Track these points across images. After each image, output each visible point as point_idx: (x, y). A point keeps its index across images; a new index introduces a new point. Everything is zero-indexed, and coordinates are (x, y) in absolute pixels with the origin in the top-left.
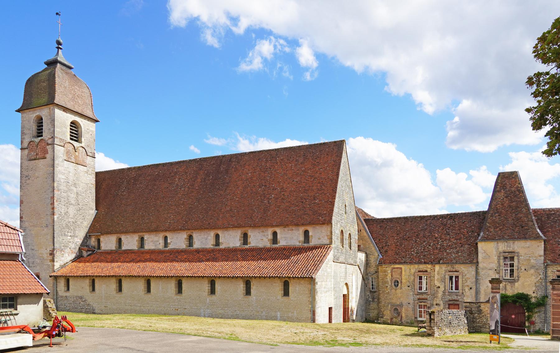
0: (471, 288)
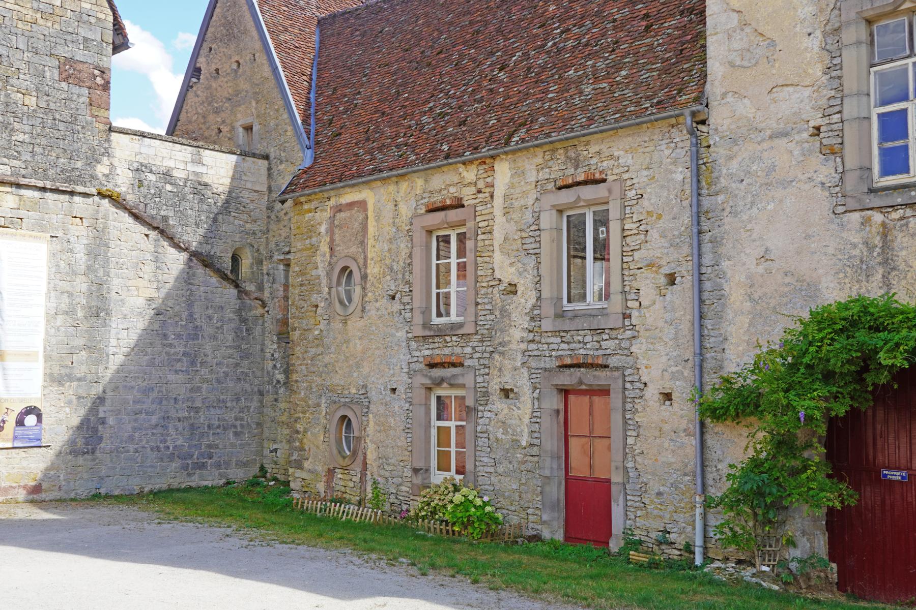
0: (671, 280)
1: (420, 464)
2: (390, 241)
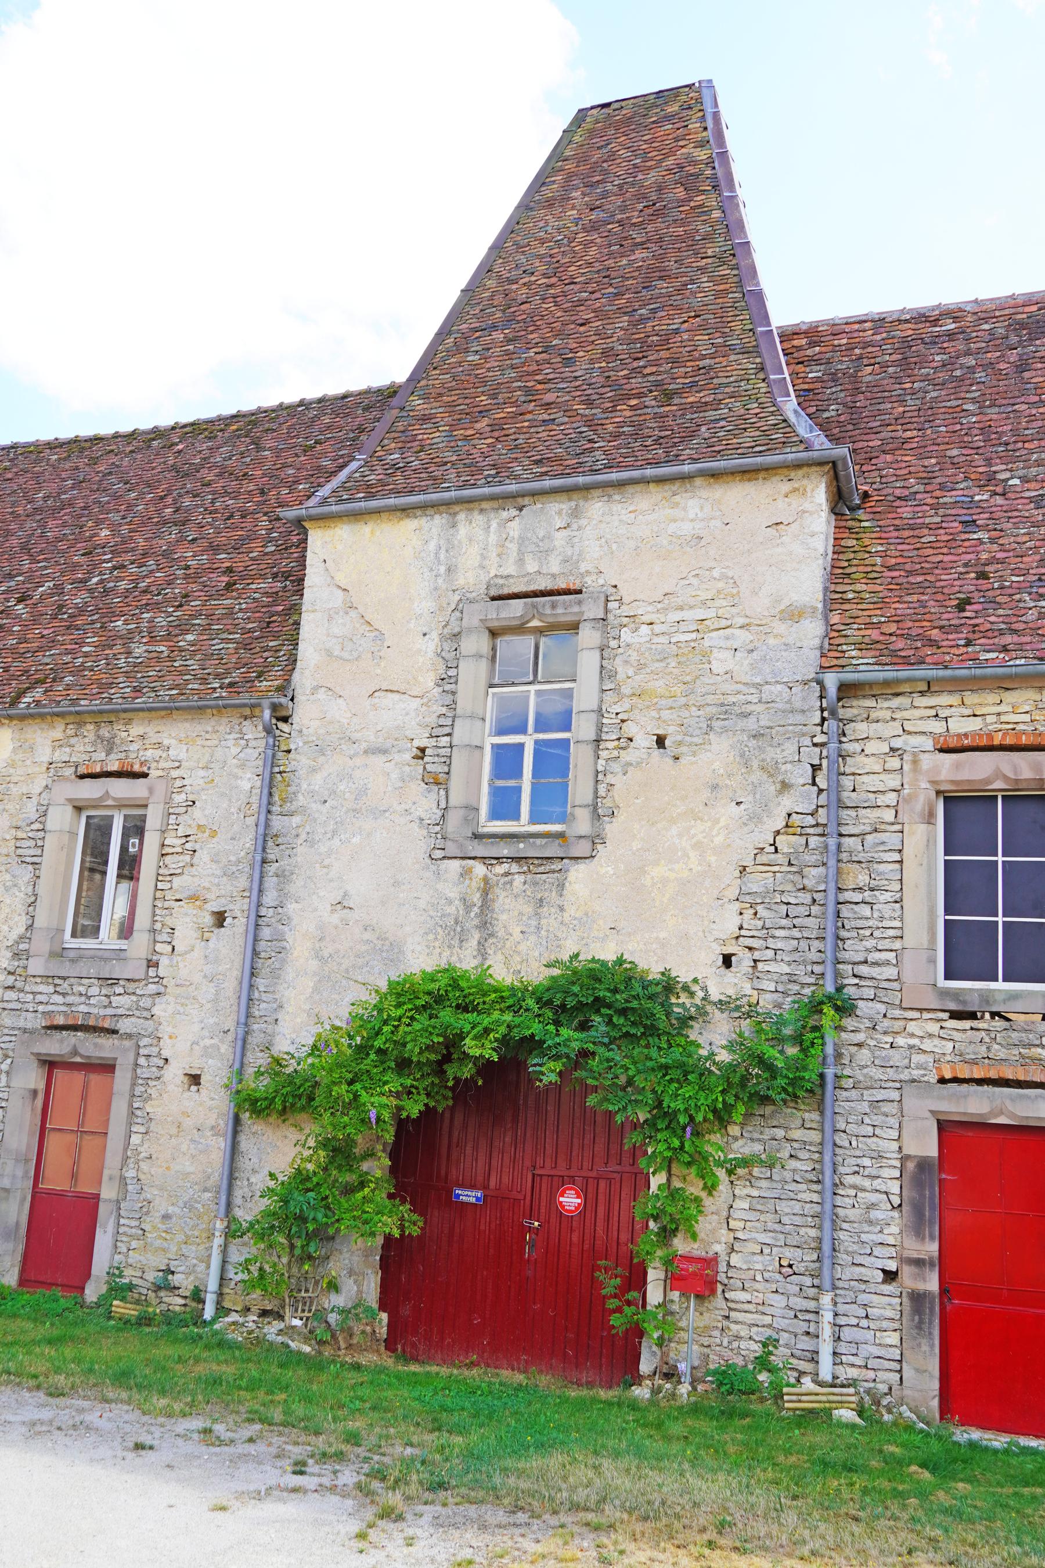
0: (220, 919)
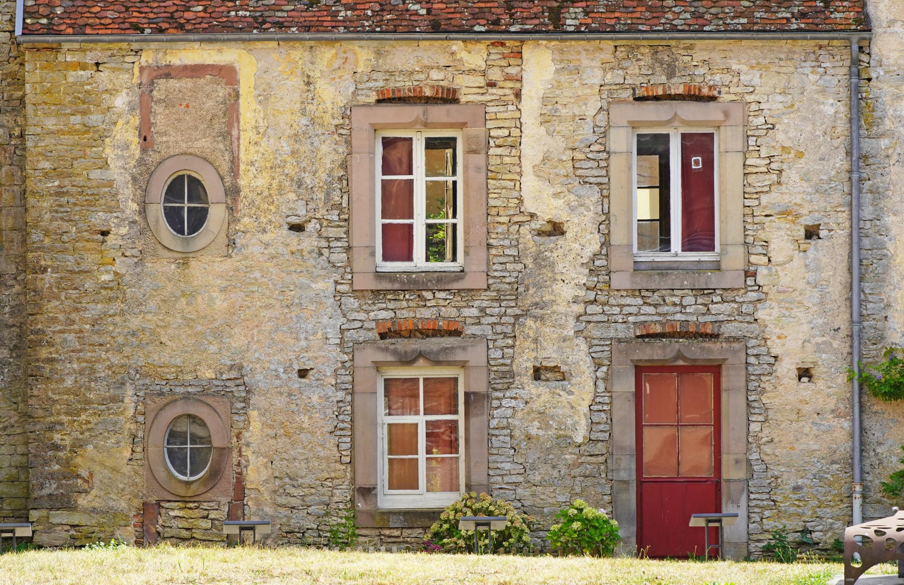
0: (811, 233)
1: (361, 482)
2: (296, 138)
